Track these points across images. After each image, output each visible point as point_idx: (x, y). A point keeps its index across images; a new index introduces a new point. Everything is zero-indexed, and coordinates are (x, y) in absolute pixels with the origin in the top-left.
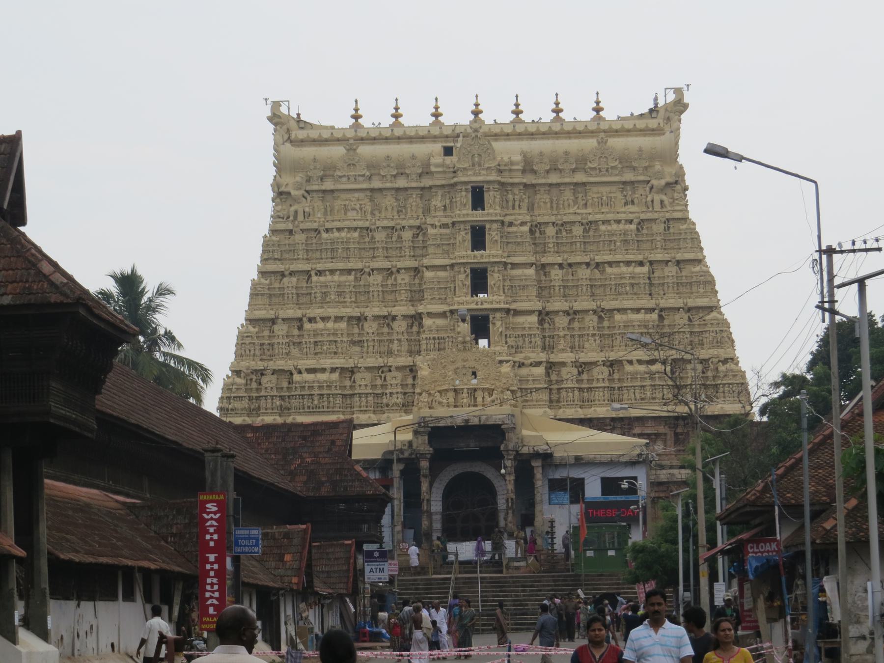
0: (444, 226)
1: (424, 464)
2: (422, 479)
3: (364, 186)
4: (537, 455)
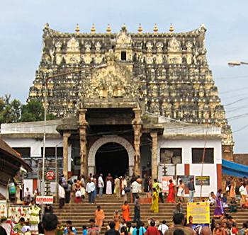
1: (82, 132)
2: (81, 143)
4: (155, 130)
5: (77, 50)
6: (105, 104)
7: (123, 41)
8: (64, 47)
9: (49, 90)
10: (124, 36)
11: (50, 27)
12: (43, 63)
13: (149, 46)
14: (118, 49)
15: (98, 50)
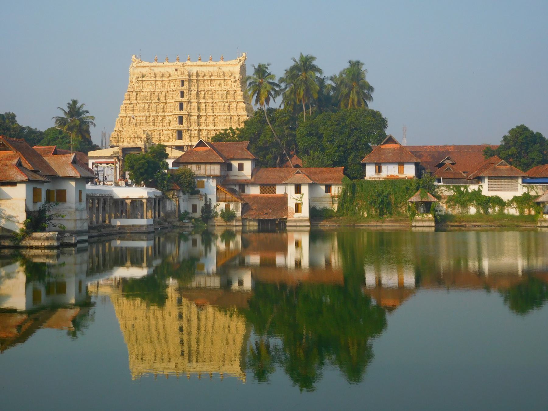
0: (173, 91)
3: (154, 79)
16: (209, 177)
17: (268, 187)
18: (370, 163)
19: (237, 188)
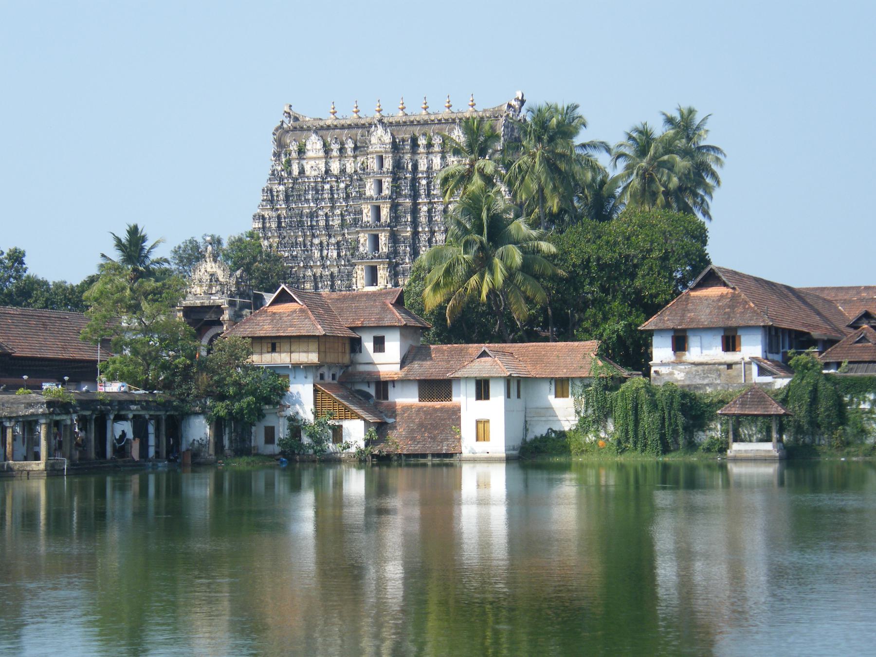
5: (321, 154)
6: (198, 303)
7: (380, 139)
8: (301, 151)
9: (279, 217)
10: (380, 130)
11: (297, 110)
12: (275, 176)
13: (422, 141)
14: (372, 153)
15: (350, 152)
16: (296, 367)
17: (437, 388)
18: (661, 331)
19: (372, 391)
